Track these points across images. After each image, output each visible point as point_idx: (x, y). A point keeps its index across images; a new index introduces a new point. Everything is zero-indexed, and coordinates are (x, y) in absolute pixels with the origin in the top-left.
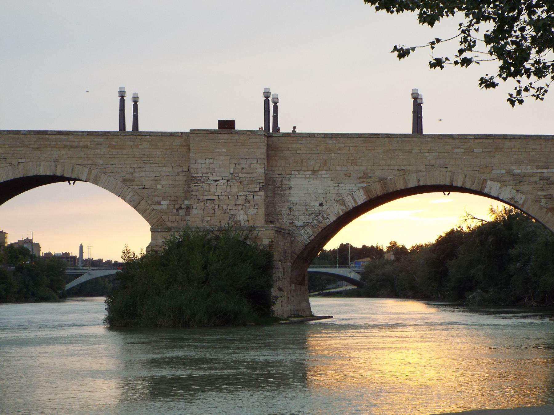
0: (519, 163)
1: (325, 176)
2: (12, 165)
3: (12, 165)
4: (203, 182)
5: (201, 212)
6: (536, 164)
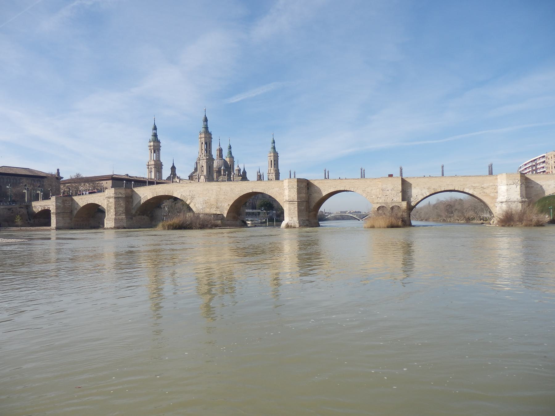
2: (334, 188)
3: (334, 188)
4: (384, 191)
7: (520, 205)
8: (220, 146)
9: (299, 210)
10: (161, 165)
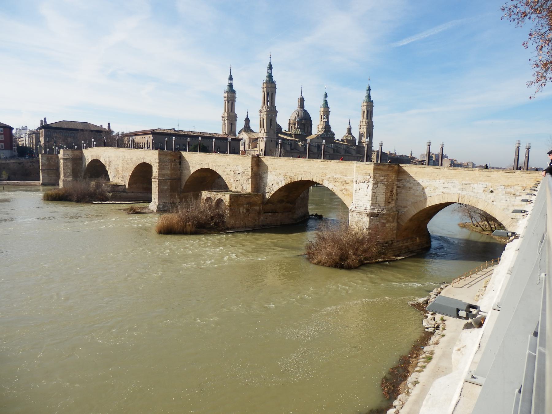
0: (336, 173)
7: (366, 219)
8: (302, 95)
9: (160, 190)
10: (235, 117)
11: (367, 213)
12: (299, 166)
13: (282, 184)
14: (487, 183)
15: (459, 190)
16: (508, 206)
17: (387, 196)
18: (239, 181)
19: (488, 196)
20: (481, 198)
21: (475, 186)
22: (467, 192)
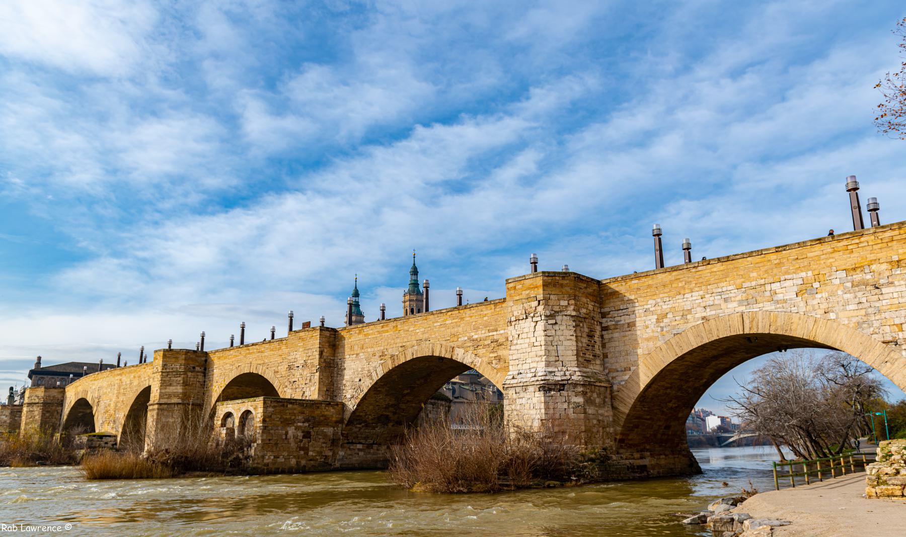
0: (476, 329)
1: (362, 357)
5: (291, 391)
6: (488, 328)
11: (538, 383)
12: (408, 331)
13: (377, 374)
14: (803, 274)
15: (740, 303)
16: (867, 315)
17: (580, 344)
18: (297, 383)
19: (810, 302)
20: (794, 309)
21: (775, 286)
22: (761, 305)
